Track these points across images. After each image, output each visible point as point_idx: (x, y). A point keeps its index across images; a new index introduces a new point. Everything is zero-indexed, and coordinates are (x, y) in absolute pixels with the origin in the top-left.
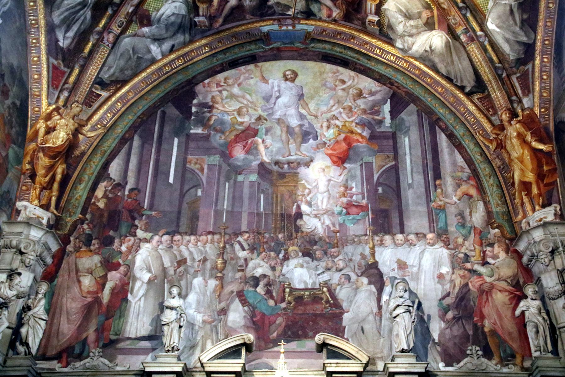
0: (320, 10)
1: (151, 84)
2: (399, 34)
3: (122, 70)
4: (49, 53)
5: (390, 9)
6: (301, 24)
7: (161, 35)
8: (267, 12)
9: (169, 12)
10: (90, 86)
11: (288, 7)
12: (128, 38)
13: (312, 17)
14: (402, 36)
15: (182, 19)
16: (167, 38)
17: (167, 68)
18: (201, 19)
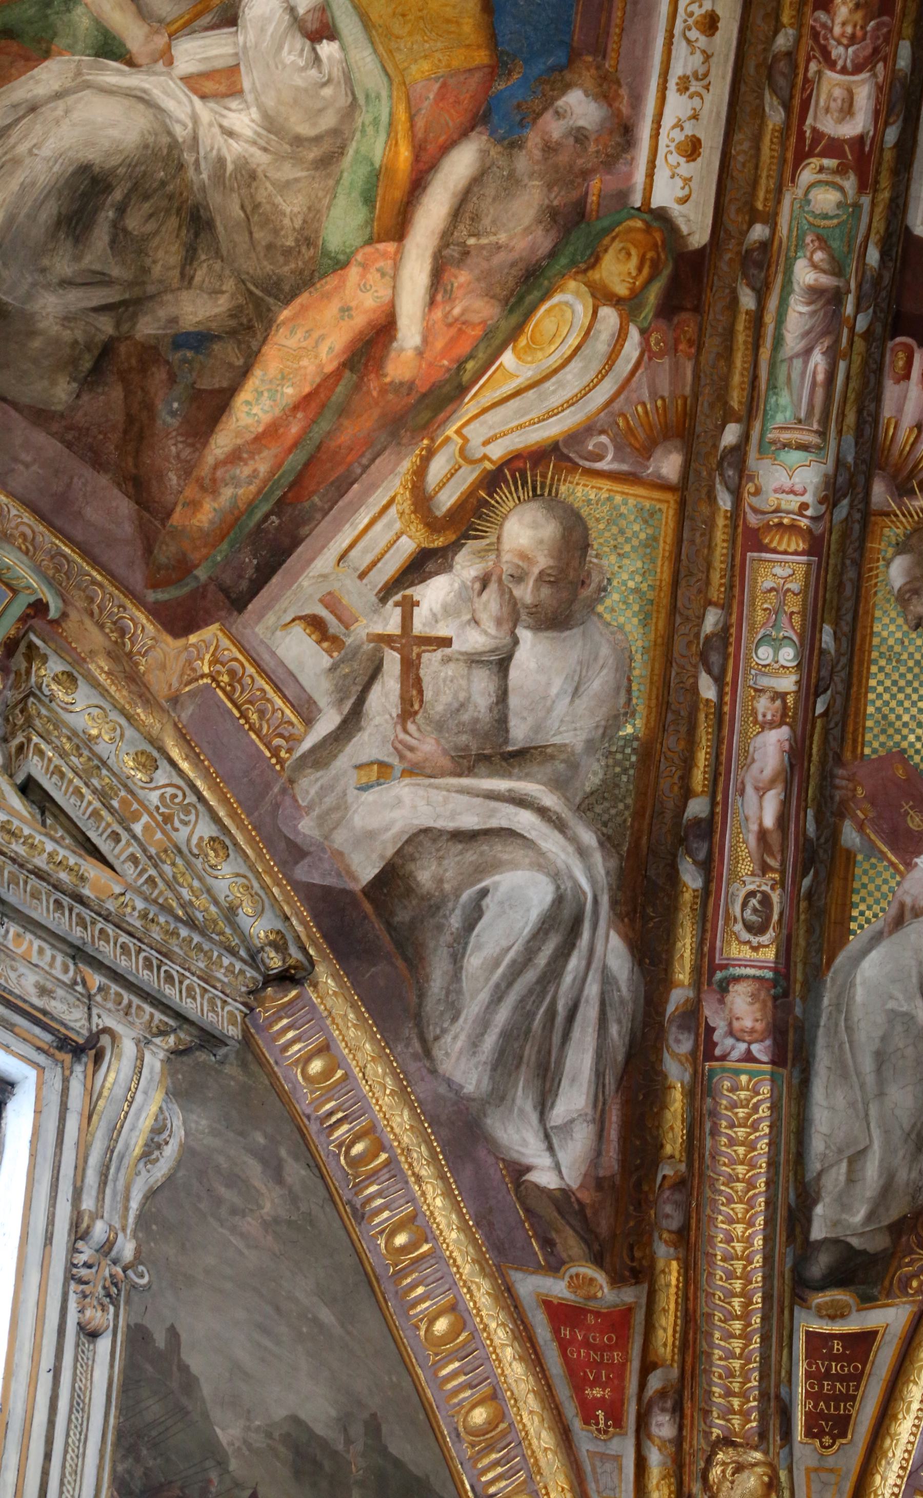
4: (501, 1255)
10: (756, 1320)
12: (874, 954)
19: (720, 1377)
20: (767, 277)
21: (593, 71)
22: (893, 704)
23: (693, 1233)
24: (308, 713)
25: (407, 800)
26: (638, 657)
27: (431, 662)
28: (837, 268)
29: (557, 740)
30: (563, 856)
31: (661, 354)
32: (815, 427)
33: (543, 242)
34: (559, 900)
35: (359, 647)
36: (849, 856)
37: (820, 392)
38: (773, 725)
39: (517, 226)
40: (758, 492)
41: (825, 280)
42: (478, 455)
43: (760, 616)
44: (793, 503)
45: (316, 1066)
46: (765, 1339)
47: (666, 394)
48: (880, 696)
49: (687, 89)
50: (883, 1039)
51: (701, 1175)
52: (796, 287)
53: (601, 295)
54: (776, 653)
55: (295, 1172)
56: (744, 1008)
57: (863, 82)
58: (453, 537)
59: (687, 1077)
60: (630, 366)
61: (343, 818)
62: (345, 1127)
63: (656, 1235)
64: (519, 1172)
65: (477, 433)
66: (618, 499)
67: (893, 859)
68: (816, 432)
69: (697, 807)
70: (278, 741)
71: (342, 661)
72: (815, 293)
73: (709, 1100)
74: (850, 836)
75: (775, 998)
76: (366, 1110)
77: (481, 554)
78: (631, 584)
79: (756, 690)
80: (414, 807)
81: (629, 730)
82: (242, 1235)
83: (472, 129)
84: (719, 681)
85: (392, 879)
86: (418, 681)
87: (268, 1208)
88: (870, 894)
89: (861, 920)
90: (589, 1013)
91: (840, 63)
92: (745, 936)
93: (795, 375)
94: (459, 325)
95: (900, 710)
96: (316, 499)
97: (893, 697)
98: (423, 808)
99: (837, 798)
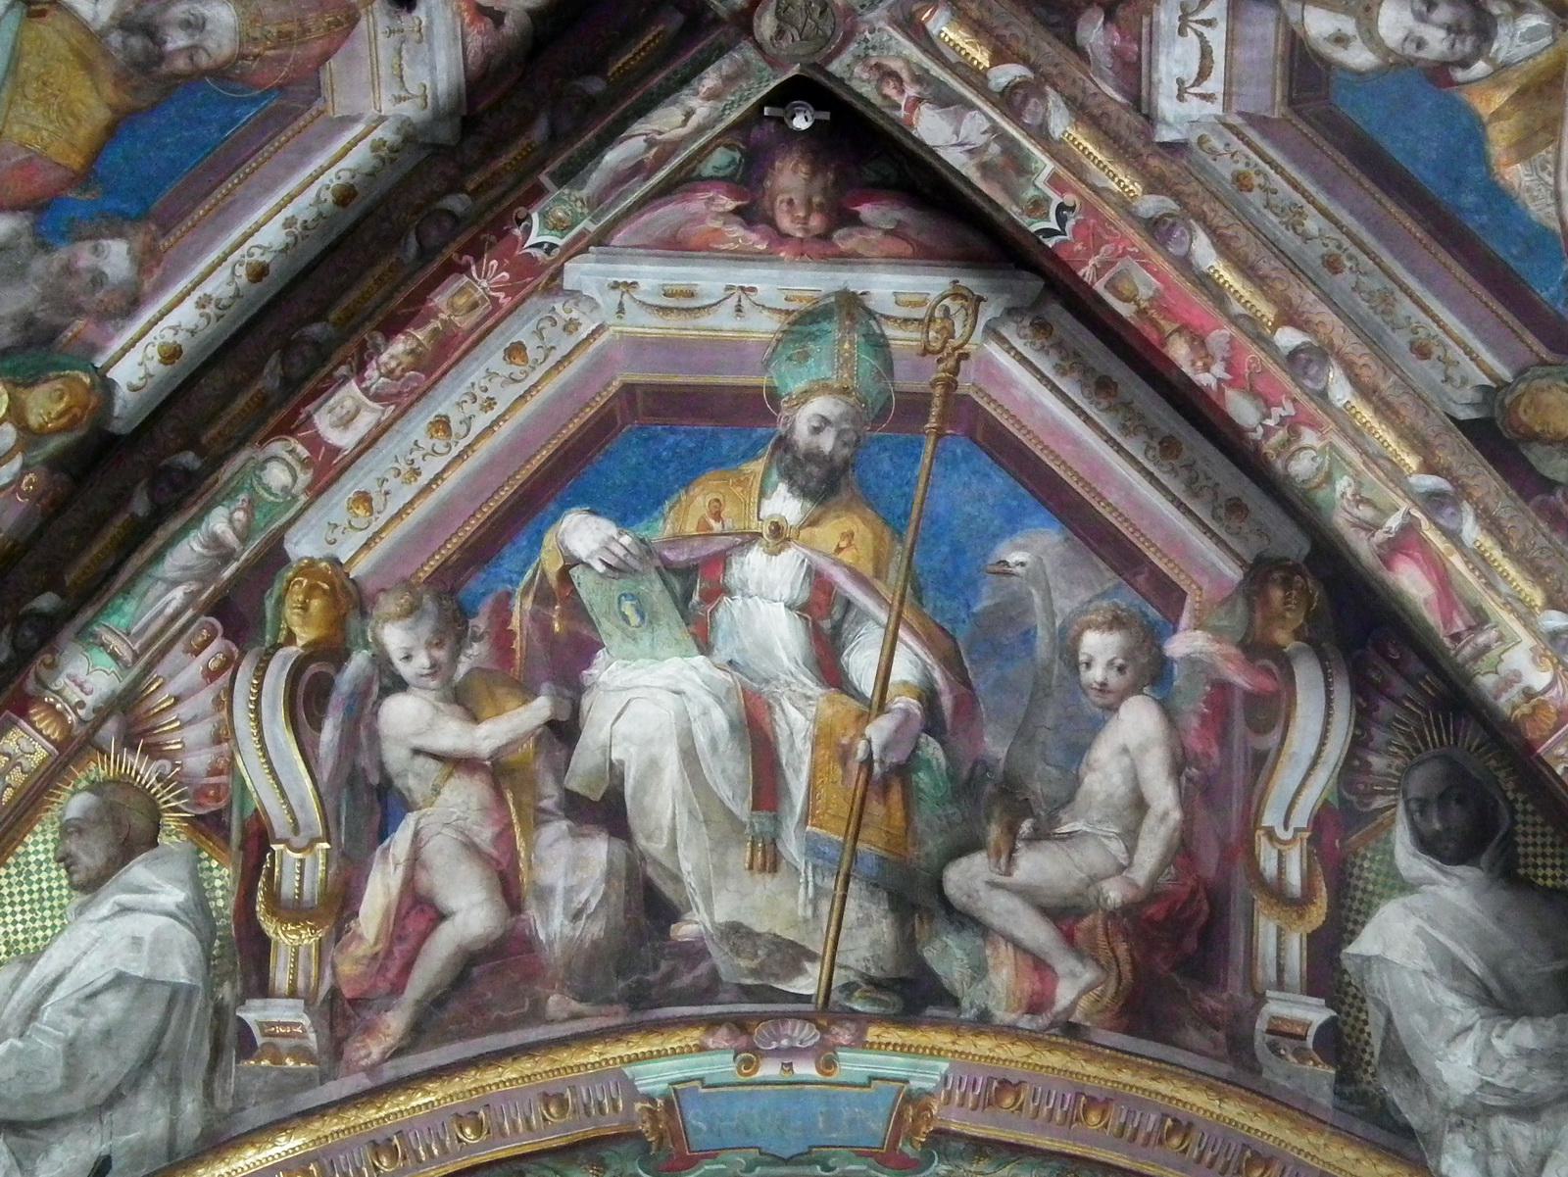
0: (979, 971)
2: (1456, 1102)
5: (1395, 956)
6: (870, 1047)
7: (34, 1098)
8: (669, 977)
9: (94, 969)
11: (794, 956)
13: (932, 1011)
14: (1472, 1115)
16: (67, 1118)
21: (148, 239)
28: (244, 538)
32: (136, 647)
37: (160, 621)
40: (53, 666)
41: (230, 538)
49: (204, 307)
52: (203, 526)
57: (373, 410)
72: (215, 541)
83: (23, 209)
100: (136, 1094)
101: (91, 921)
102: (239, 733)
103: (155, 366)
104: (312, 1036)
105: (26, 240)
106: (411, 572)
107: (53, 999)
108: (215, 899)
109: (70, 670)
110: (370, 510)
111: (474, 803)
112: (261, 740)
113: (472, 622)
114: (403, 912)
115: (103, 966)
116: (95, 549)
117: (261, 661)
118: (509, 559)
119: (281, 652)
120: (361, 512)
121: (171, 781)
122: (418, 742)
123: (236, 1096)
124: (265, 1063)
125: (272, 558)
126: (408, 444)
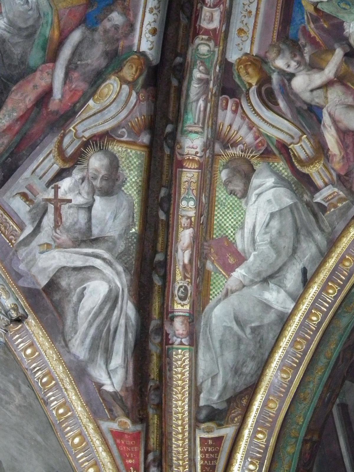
1: (299, 364)
3: (236, 371)
4: (95, 415)
9: (262, 218)
10: (186, 434)
12: (218, 306)
15: (293, 213)
16: (285, 264)
17: (314, 318)
18: (326, 192)
19: (175, 454)
20: (183, 75)
21: (121, 6)
22: (223, 220)
23: (163, 405)
24: (22, 228)
25: (57, 256)
26: (136, 205)
27: (65, 208)
28: (207, 72)
29: (109, 234)
30: (111, 275)
31: (143, 101)
32: (200, 125)
33: (103, 63)
34: (110, 291)
35: (39, 203)
36: (209, 273)
37: (202, 114)
38: (187, 228)
39: (95, 58)
40: (181, 148)
41: (204, 76)
42: (81, 136)
43: (183, 191)
44: (193, 151)
45: (29, 351)
46: (190, 440)
47: (145, 114)
48: (218, 217)
49: (152, 12)
50: (222, 335)
51: (166, 385)
52: (193, 78)
53: (123, 81)
54: (188, 203)
55: (24, 388)
56: (179, 327)
57: (217, 10)
58: (72, 164)
59: (158, 351)
60: (133, 105)
61: (35, 263)
62: (40, 372)
63: (149, 406)
64: (99, 386)
65: (80, 128)
66: (129, 150)
67: (224, 273)
68: (200, 127)
69: (159, 257)
70: (11, 237)
71: (33, 208)
72: (200, 80)
73: (168, 359)
74: (209, 266)
75: (190, 323)
76: (47, 366)
77: (82, 170)
78: (133, 180)
79: (181, 216)
80: (60, 259)
81: (134, 230)
82: (10, 411)
83: (80, 25)
84: (167, 213)
85: (52, 286)
86: (60, 215)
87: (17, 400)
88: (217, 286)
89: (214, 295)
90: (121, 330)
91: (209, 4)
92: (179, 301)
93: (194, 108)
94: (74, 91)
95: (225, 222)
96: (24, 152)
97: (223, 218)
98: (63, 259)
99: (205, 253)
100: (300, 244)
101: (252, 205)
102: (255, 122)
103: (152, 38)
104: (341, 193)
105: (87, 33)
106: (270, 41)
107: (257, 234)
108: (283, 174)
109: (186, 145)
110: (245, 33)
111: (340, 93)
112: (263, 120)
113: (299, 43)
114: (342, 139)
115: (264, 215)
116: (172, 104)
117: (246, 97)
118: (297, 17)
119: (250, 91)
120: (243, 35)
121: (246, 149)
122: (310, 88)
123: (331, 225)
124: (332, 210)
125: (227, 67)
126: (242, 5)
